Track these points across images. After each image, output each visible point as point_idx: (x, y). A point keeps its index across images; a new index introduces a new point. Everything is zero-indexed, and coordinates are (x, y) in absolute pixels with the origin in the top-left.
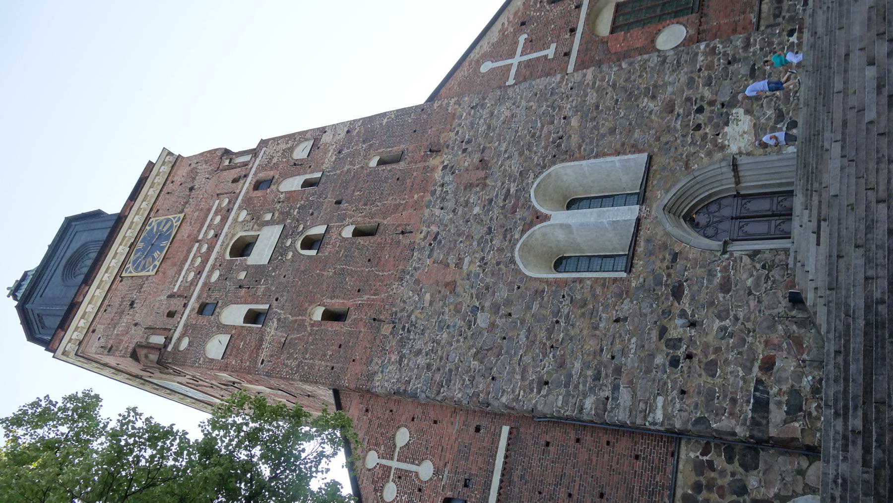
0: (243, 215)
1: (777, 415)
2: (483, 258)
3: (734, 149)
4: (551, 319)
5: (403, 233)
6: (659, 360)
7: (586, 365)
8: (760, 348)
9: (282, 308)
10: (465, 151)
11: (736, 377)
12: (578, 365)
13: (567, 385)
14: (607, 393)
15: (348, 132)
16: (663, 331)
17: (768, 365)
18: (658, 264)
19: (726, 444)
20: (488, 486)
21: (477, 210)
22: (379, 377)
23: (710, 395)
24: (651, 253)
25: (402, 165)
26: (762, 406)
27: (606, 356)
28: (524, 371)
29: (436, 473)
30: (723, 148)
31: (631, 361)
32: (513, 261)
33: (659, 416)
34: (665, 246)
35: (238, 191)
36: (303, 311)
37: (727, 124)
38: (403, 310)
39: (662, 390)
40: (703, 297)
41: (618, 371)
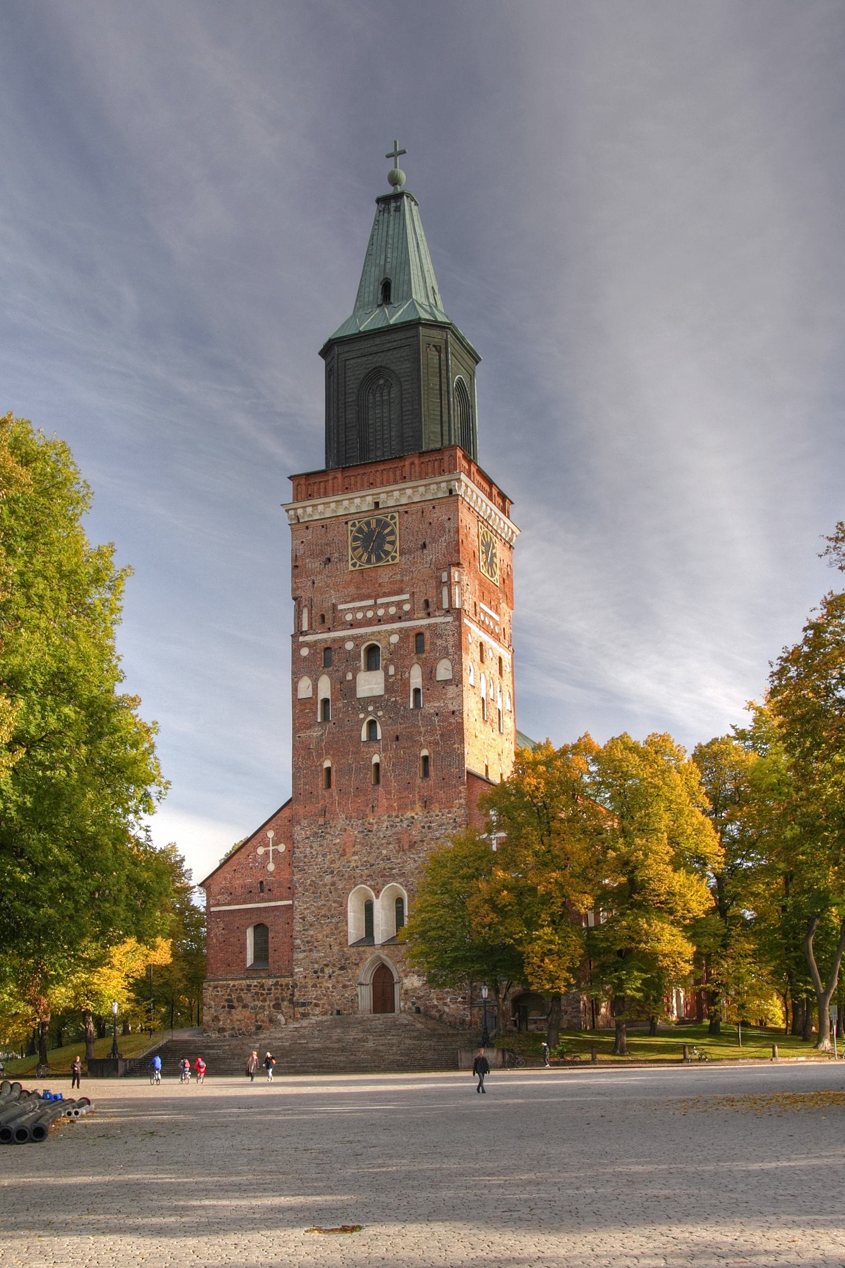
0: (394, 639)
1: (301, 1010)
2: (357, 867)
3: (405, 981)
4: (329, 914)
5: (373, 807)
6: (316, 966)
7: (312, 936)
8: (322, 1002)
9: (329, 733)
10: (423, 827)
11: (312, 994)
12: (312, 933)
13: (304, 930)
14: (303, 948)
15: (453, 712)
16: (327, 965)
17: (316, 1005)
18: (354, 958)
19: (292, 995)
20: (270, 901)
21: (384, 852)
22: (299, 827)
23: (306, 987)
24: (359, 954)
25: (419, 781)
26: (303, 1005)
27: (316, 944)
28: (307, 908)
29: (271, 873)
30: (406, 976)
31: (315, 955)
32: (356, 885)
33: (296, 970)
34: (361, 959)
35: (415, 617)
36: (328, 753)
37: (419, 976)
38: (331, 827)
39: (305, 970)
40: (340, 978)
41: (311, 950)
